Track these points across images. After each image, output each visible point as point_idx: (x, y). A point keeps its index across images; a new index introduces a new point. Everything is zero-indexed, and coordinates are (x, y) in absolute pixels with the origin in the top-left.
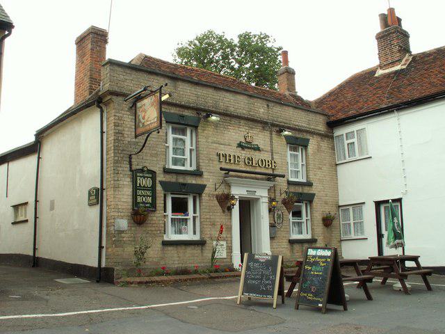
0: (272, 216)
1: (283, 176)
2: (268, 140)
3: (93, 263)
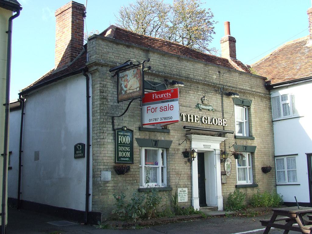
0: (223, 166)
1: (232, 133)
2: (219, 101)
3: (82, 208)
